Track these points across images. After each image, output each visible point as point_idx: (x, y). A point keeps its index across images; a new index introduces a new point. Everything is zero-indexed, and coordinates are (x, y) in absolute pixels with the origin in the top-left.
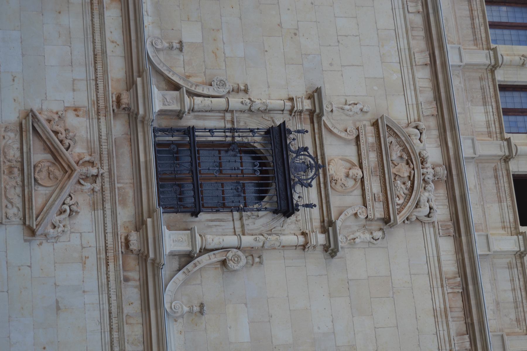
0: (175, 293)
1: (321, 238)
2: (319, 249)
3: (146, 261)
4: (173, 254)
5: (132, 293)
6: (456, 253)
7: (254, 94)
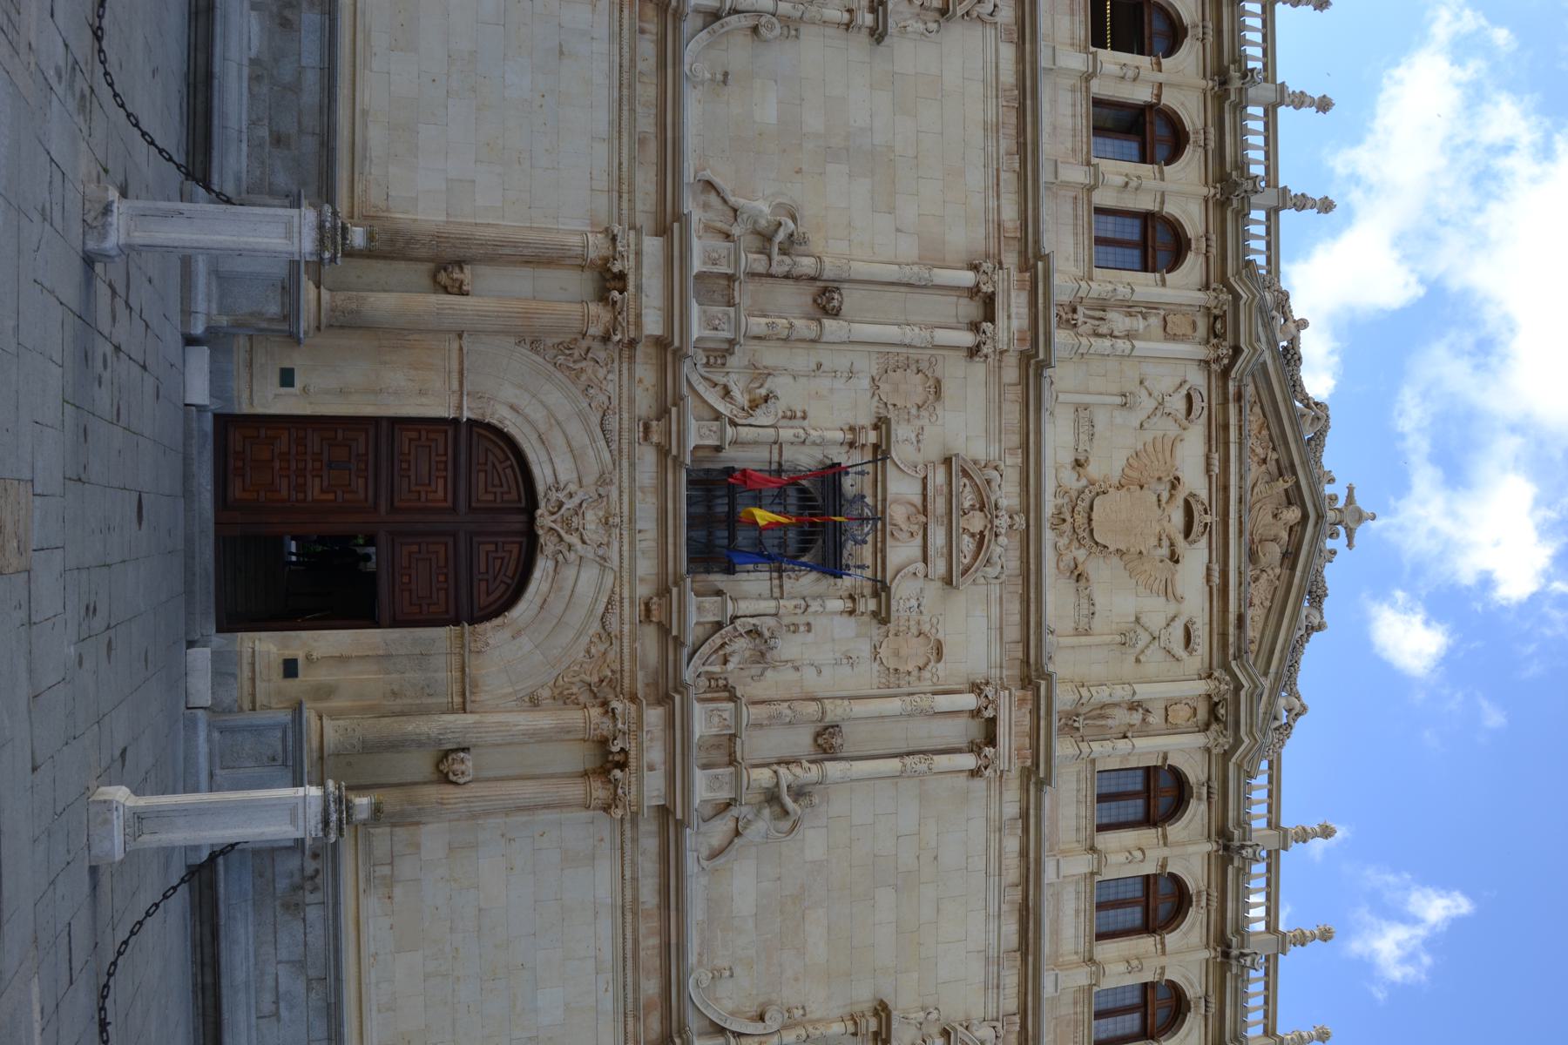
0: (697, 52)
1: (869, 19)
2: (865, 32)
3: (666, 11)
4: (697, 11)
6: (1017, 63)
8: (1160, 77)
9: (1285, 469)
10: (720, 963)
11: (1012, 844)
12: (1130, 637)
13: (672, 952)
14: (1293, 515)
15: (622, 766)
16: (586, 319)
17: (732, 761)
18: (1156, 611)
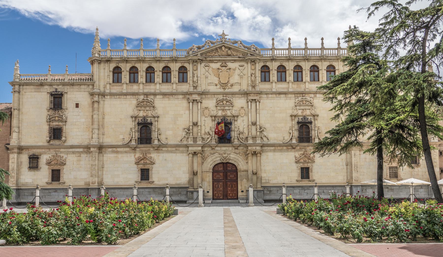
1: (156, 118)
5: (164, 149)
7: (131, 127)
8: (158, 71)
9: (216, 49)
10: (282, 139)
11: (270, 96)
12: (241, 76)
13: (280, 145)
14: (223, 48)
15: (255, 152)
16: (200, 157)
17: (256, 137)
18: (237, 72)
